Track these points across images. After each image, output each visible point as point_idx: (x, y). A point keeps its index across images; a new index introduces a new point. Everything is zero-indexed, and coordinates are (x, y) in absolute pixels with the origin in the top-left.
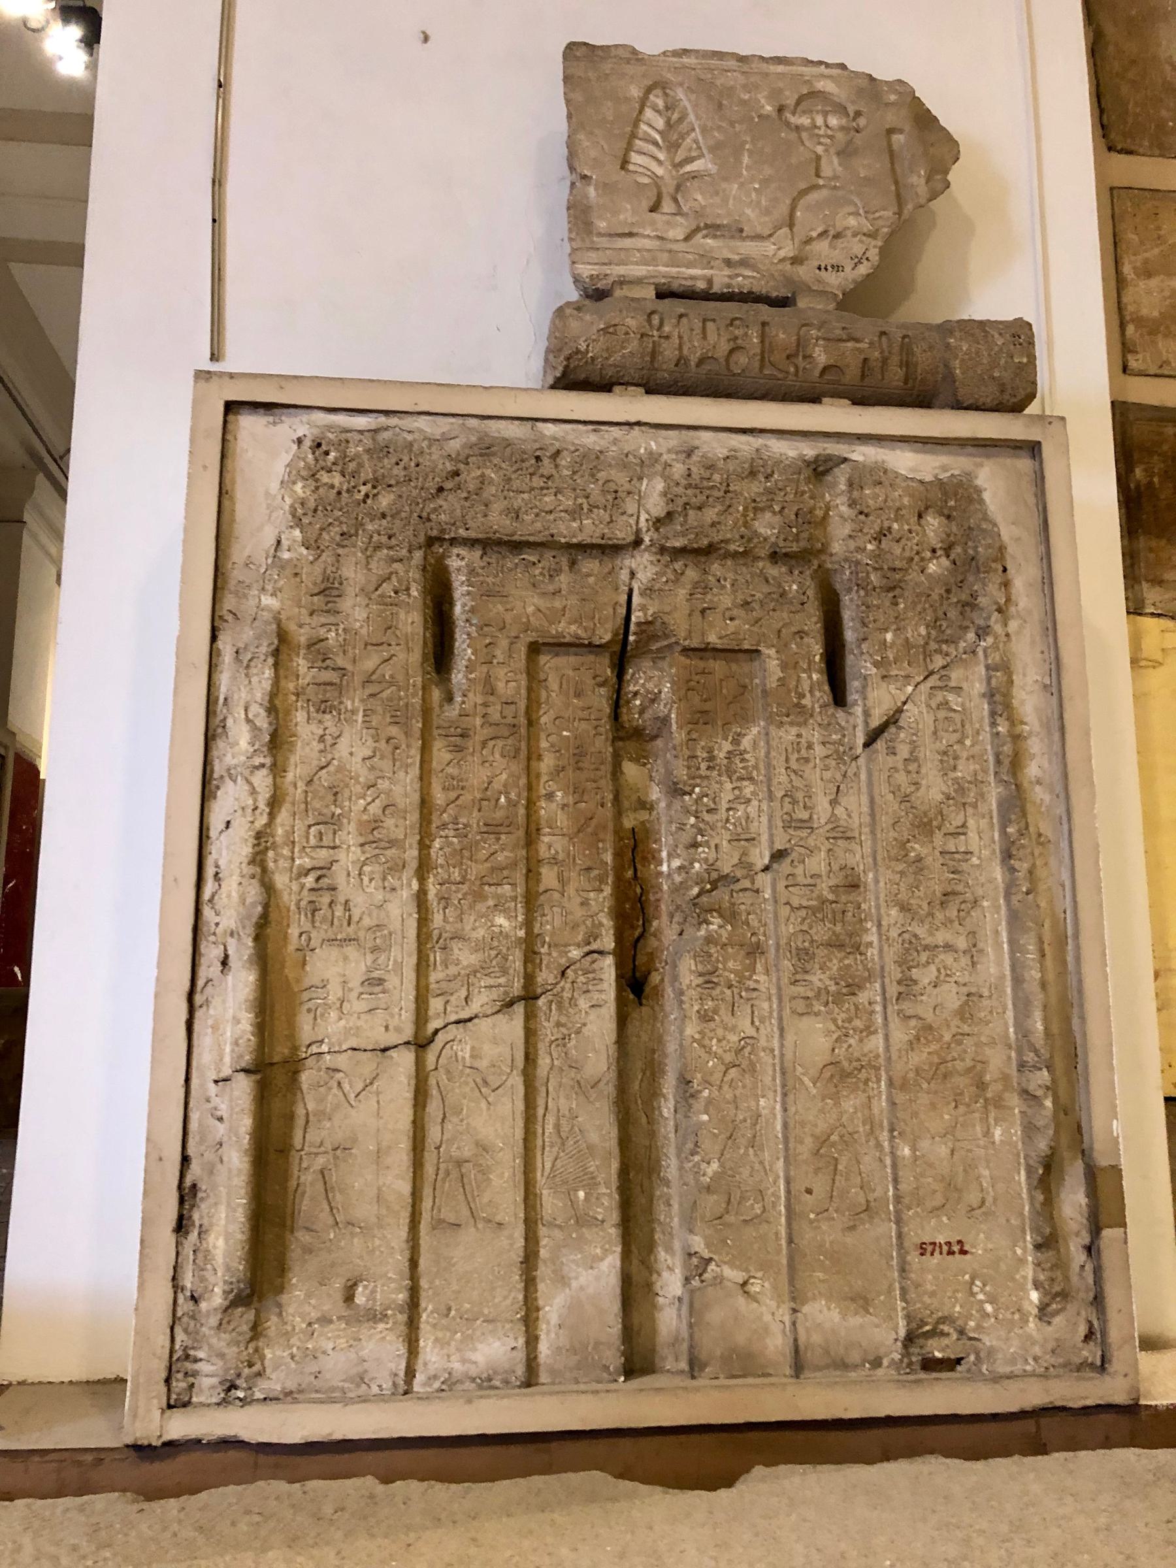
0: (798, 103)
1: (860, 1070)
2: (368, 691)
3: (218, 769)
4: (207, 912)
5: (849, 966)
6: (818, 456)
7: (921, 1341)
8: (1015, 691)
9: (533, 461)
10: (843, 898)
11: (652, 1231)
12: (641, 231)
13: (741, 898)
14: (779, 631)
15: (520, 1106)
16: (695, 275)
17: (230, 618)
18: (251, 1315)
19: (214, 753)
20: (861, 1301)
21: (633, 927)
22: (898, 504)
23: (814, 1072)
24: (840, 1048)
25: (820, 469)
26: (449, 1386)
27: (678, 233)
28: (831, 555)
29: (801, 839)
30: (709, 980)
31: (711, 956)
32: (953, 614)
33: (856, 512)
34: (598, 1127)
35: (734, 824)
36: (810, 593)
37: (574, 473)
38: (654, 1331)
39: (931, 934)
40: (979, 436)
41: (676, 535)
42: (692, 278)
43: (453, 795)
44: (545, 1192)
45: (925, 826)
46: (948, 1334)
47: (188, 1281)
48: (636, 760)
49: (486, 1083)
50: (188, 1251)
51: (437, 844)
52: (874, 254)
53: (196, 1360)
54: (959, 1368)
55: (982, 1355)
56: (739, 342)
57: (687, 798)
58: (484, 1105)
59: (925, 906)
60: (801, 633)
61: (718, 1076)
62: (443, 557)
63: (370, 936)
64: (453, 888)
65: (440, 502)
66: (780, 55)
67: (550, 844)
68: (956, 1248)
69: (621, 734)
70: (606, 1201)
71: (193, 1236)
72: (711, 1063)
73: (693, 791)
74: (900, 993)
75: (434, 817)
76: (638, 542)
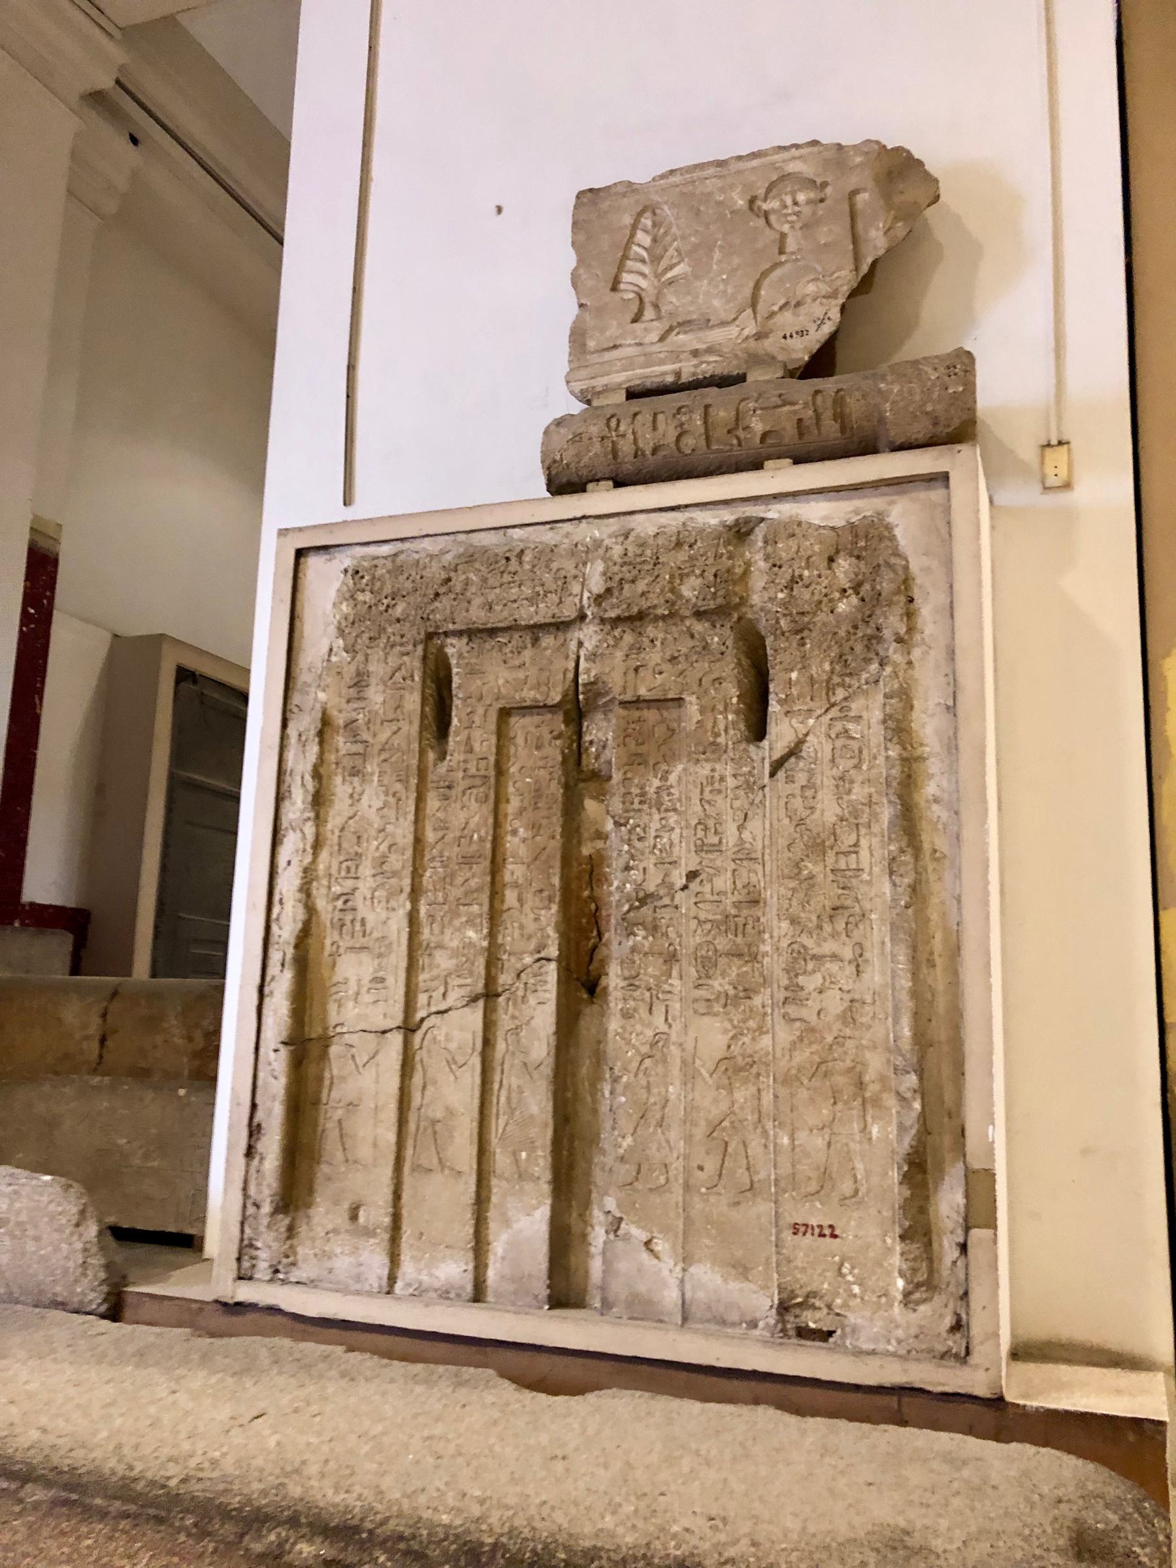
0: (769, 190)
1: (752, 1066)
2: (383, 757)
3: (285, 823)
4: (275, 928)
5: (746, 972)
6: (737, 520)
7: (797, 1311)
8: (915, 715)
9: (504, 561)
10: (745, 912)
11: (590, 1192)
12: (623, 342)
13: (666, 914)
14: (700, 680)
15: (478, 1080)
16: (663, 371)
17: (295, 710)
18: (287, 1221)
19: (283, 811)
20: (742, 1269)
21: (589, 939)
22: (810, 553)
23: (711, 1065)
24: (736, 1045)
25: (741, 532)
26: (419, 1293)
27: (654, 336)
28: (752, 606)
29: (711, 860)
30: (632, 983)
31: (634, 962)
32: (859, 648)
33: (769, 565)
34: (538, 1103)
35: (661, 851)
36: (729, 643)
37: (534, 566)
38: (587, 1273)
39: (819, 945)
40: (887, 477)
41: (613, 607)
42: (664, 374)
43: (440, 834)
44: (498, 1151)
45: (818, 847)
46: (820, 1309)
47: (252, 1190)
48: (595, 798)
49: (455, 1063)
50: (253, 1170)
51: (428, 874)
52: (835, 314)
53: (257, 1249)
54: (831, 1340)
55: (848, 1330)
56: (685, 426)
57: (623, 828)
58: (452, 1078)
59: (814, 918)
60: (719, 680)
61: (635, 1065)
62: (442, 647)
63: (377, 945)
64: (438, 907)
65: (437, 604)
66: (755, 150)
67: (513, 871)
68: (827, 1232)
69: (582, 776)
70: (541, 1162)
71: (256, 1162)
72: (629, 1054)
73: (628, 822)
74: (786, 998)
75: (426, 852)
76: (582, 617)
